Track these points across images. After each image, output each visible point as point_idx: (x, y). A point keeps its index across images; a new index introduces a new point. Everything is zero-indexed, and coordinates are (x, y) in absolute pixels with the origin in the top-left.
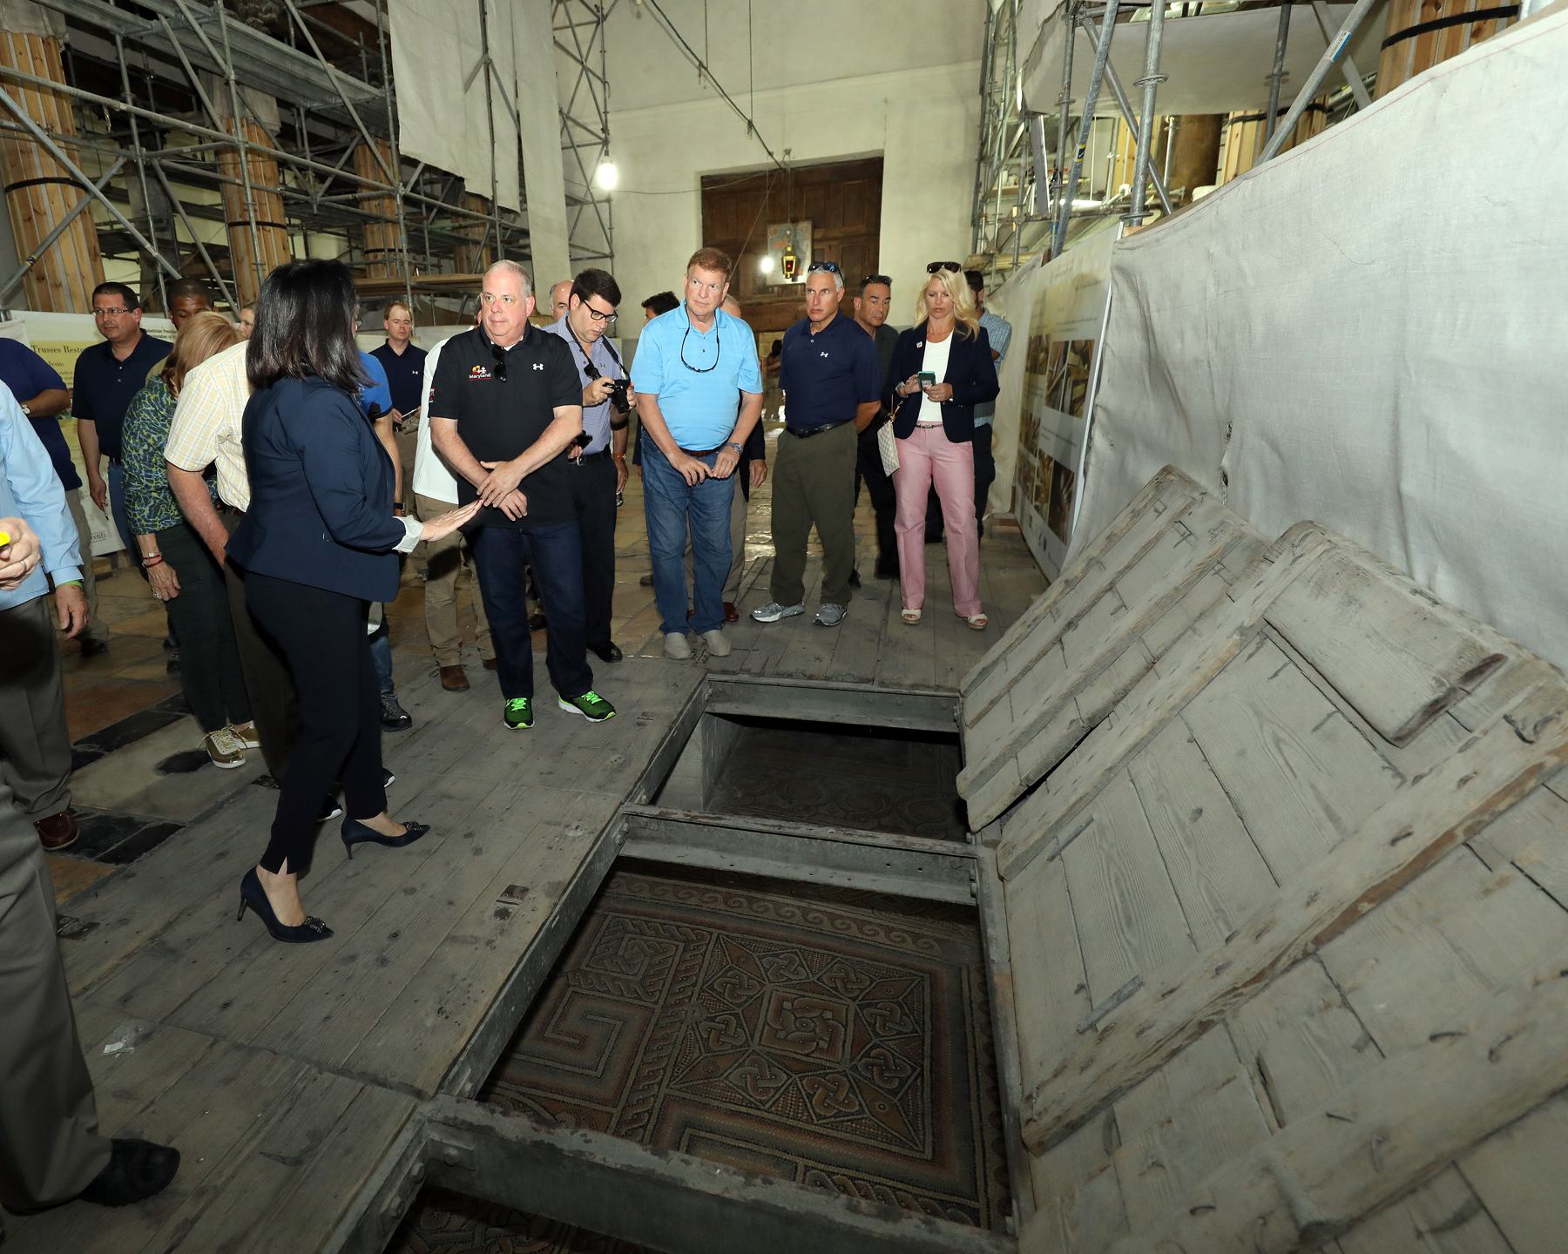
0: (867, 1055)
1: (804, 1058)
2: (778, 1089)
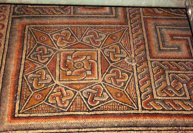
0: (49, 58)
1: (77, 49)
2: (85, 35)
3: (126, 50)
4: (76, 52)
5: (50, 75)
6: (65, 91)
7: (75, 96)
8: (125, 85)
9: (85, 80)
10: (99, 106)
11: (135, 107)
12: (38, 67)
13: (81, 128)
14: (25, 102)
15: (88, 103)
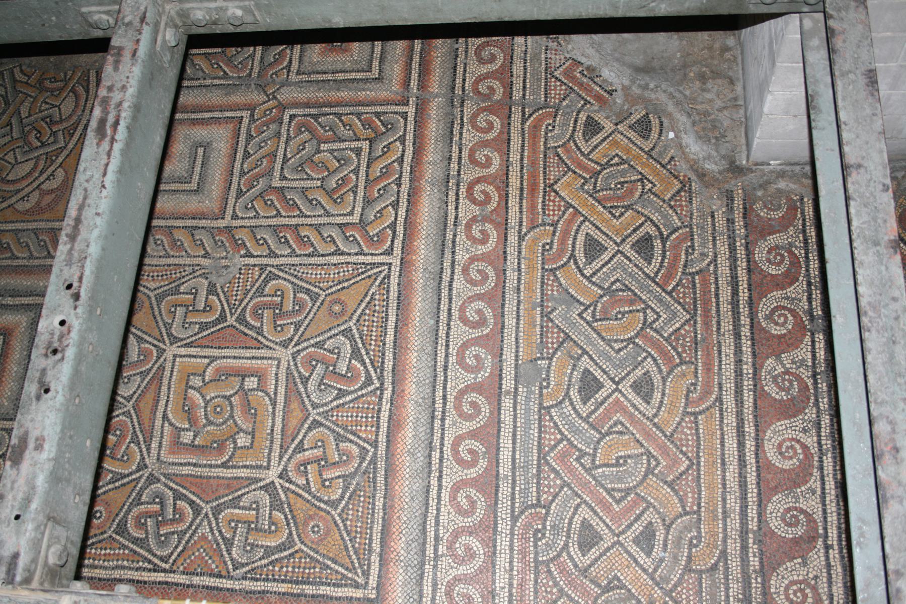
0: (178, 496)
1: (159, 415)
3: (183, 277)
4: (170, 416)
5: (244, 494)
6: (307, 453)
7: (328, 423)
8: (308, 290)
9: (275, 394)
10: (367, 361)
11: (380, 272)
12: (208, 530)
13: (434, 411)
14: (331, 569)
15: (356, 391)
